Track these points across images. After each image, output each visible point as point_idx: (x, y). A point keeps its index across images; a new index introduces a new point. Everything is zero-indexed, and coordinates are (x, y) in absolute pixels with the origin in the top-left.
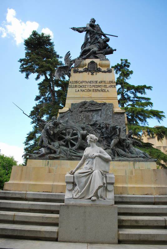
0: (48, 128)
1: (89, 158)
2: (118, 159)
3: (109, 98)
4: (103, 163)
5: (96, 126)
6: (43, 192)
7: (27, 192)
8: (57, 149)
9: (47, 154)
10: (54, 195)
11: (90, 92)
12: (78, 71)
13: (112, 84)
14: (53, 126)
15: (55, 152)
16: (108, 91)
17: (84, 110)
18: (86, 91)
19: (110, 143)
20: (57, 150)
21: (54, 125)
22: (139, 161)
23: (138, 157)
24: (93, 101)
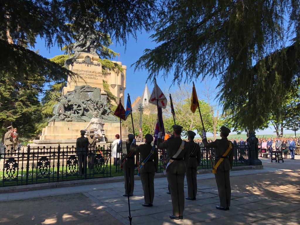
12: (78, 62)
13: (100, 74)
15: (69, 117)
17: (83, 91)
22: (114, 122)
24: (89, 86)
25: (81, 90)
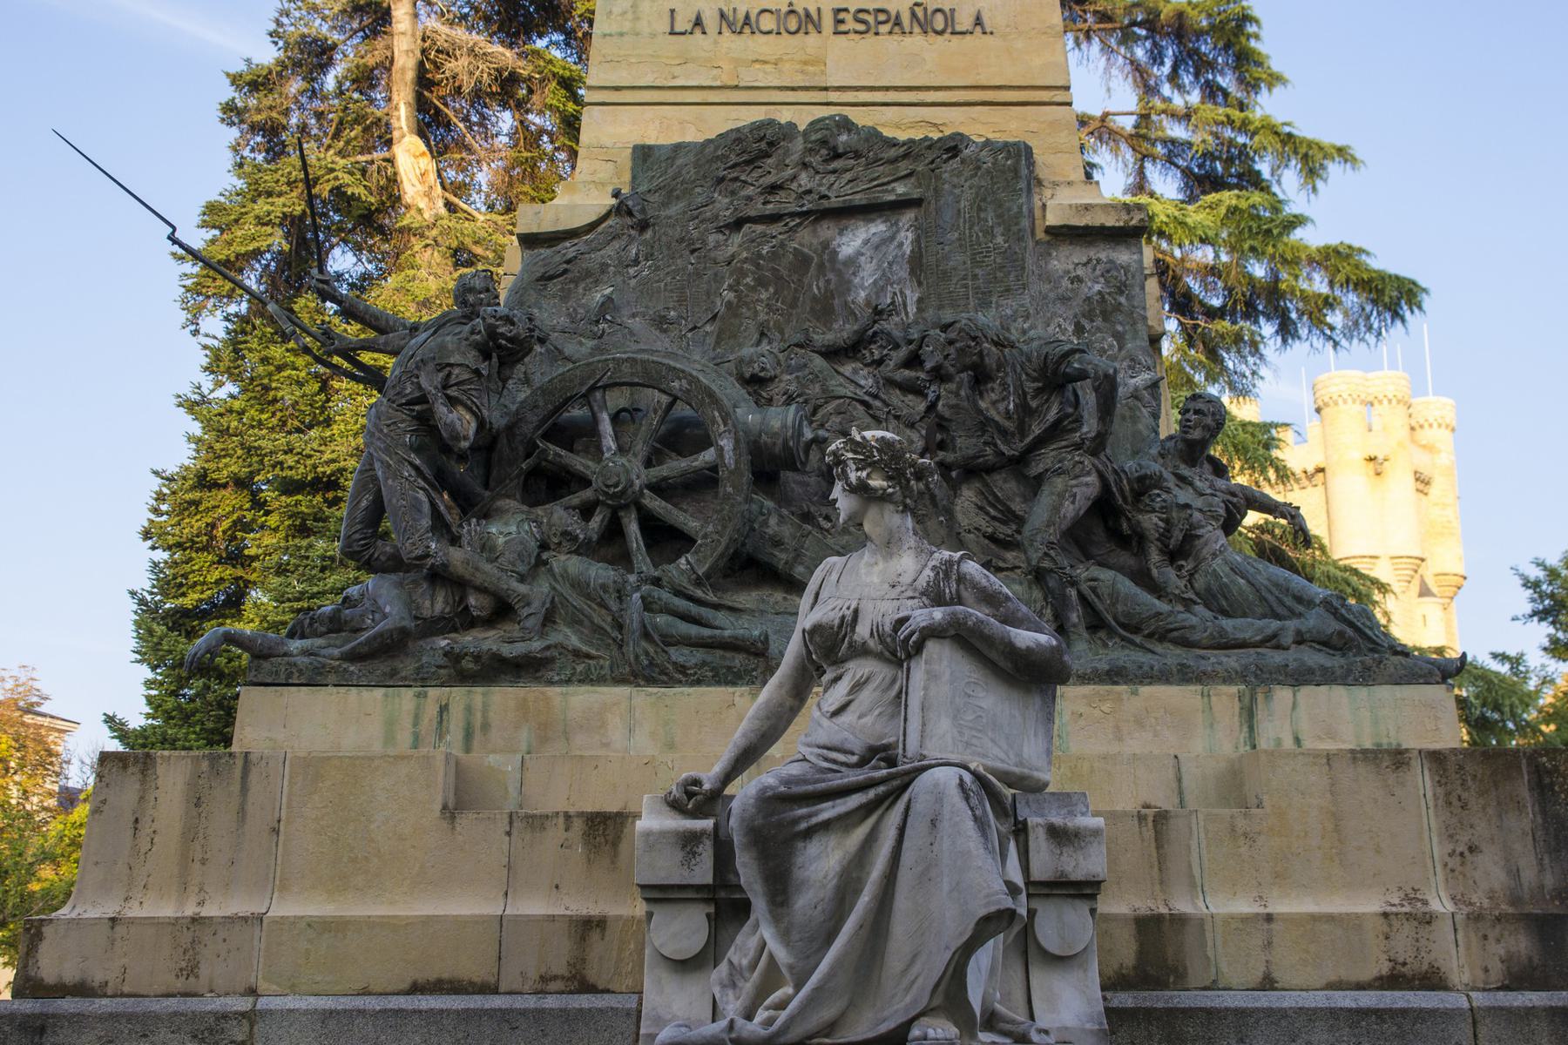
0: (429, 382)
1: (862, 651)
2: (1104, 666)
3: (990, 97)
4: (993, 700)
5: (879, 363)
6: (416, 989)
7: (262, 1003)
8: (522, 579)
9: (434, 626)
10: (523, 1013)
11: (812, 40)
14: (471, 358)
15: (503, 610)
16: (978, 21)
18: (767, 23)
19: (1020, 521)
20: (523, 588)
21: (486, 356)
22: (1300, 677)
23: (1288, 639)
24: (846, 125)
25: (723, 206)
